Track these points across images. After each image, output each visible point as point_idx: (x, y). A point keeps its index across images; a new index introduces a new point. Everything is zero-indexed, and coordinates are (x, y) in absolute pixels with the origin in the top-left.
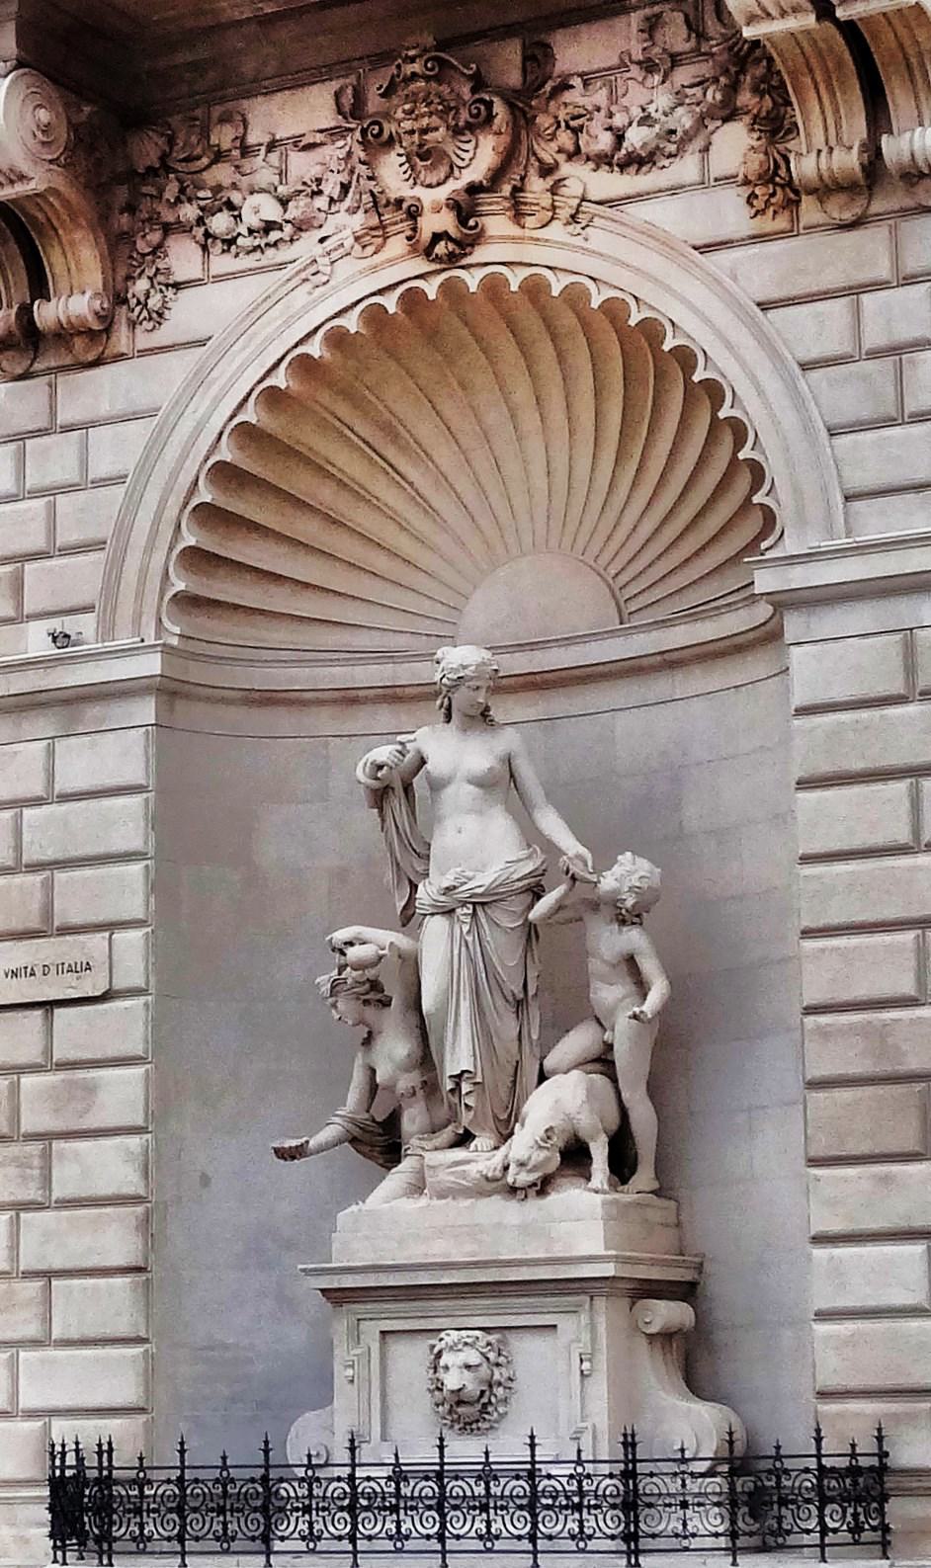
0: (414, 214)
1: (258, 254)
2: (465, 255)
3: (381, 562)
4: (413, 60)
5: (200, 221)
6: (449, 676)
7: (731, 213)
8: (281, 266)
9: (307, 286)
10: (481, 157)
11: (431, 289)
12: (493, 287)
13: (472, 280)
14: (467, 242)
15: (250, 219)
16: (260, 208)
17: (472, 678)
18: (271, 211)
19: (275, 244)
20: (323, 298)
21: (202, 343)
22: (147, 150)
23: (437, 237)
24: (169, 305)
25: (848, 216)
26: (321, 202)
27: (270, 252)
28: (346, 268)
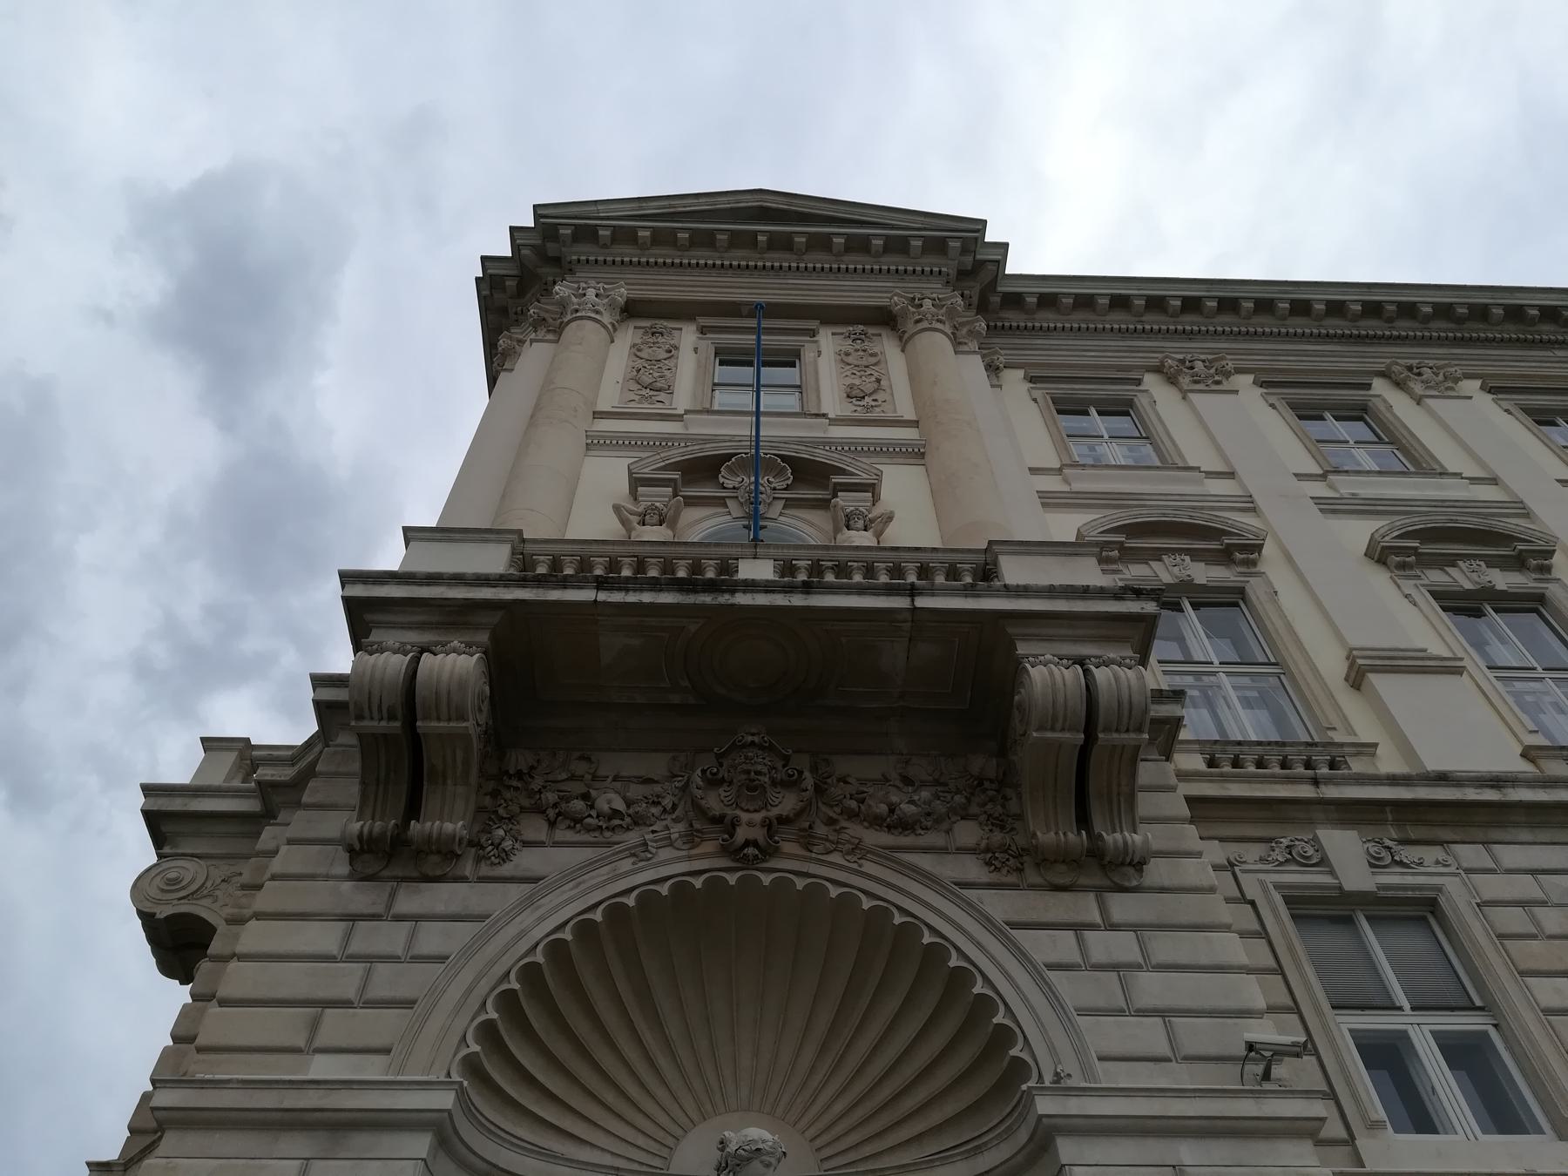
0: (734, 824)
1: (597, 834)
3: (610, 1097)
4: (753, 735)
5: (555, 805)
6: (745, 1148)
7: (973, 869)
8: (610, 844)
9: (632, 860)
10: (786, 803)
14: (768, 851)
15: (603, 804)
16: (609, 800)
17: (768, 1153)
18: (619, 805)
19: (613, 829)
20: (641, 870)
21: (535, 880)
22: (519, 759)
23: (747, 843)
24: (516, 852)
26: (655, 810)
27: (607, 834)
28: (665, 854)
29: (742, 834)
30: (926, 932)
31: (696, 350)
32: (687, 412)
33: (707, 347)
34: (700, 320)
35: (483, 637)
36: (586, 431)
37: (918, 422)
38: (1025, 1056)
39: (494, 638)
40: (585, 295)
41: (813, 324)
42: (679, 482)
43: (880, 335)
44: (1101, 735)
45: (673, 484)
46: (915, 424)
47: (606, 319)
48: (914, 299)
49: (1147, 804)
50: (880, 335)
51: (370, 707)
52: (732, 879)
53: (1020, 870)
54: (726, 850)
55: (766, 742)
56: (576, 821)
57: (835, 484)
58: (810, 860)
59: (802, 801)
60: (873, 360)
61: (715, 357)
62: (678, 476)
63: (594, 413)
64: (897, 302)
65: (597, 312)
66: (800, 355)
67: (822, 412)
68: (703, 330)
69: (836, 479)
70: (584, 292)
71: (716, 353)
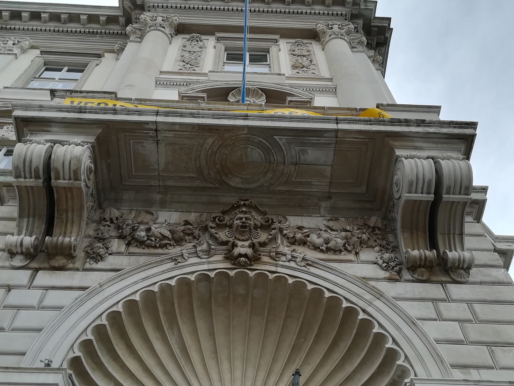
2: (251, 265)
11: (232, 273)
12: (262, 276)
13: (251, 274)
23: (240, 255)
25: (424, 278)
29: (237, 251)
30: (344, 301)
31: (215, 47)
32: (210, 72)
33: (221, 46)
34: (217, 34)
35: (92, 139)
36: (156, 78)
37: (332, 79)
38: (406, 365)
39: (98, 139)
40: (156, 20)
41: (277, 37)
42: (206, 98)
43: (311, 43)
44: (444, 196)
45: (202, 99)
46: (331, 80)
47: (167, 31)
48: (328, 25)
49: (469, 242)
50: (311, 43)
51: (24, 171)
52: (232, 273)
53: (399, 272)
54: (230, 257)
55: (253, 204)
56: (141, 243)
57: (290, 101)
58: (276, 266)
59: (271, 235)
60: (308, 53)
61: (225, 52)
62: (205, 95)
63: (161, 72)
64: (321, 26)
65: (164, 28)
66: (269, 52)
67: (282, 73)
68: (218, 39)
69: (289, 99)
70: (156, 18)
71: (225, 50)
